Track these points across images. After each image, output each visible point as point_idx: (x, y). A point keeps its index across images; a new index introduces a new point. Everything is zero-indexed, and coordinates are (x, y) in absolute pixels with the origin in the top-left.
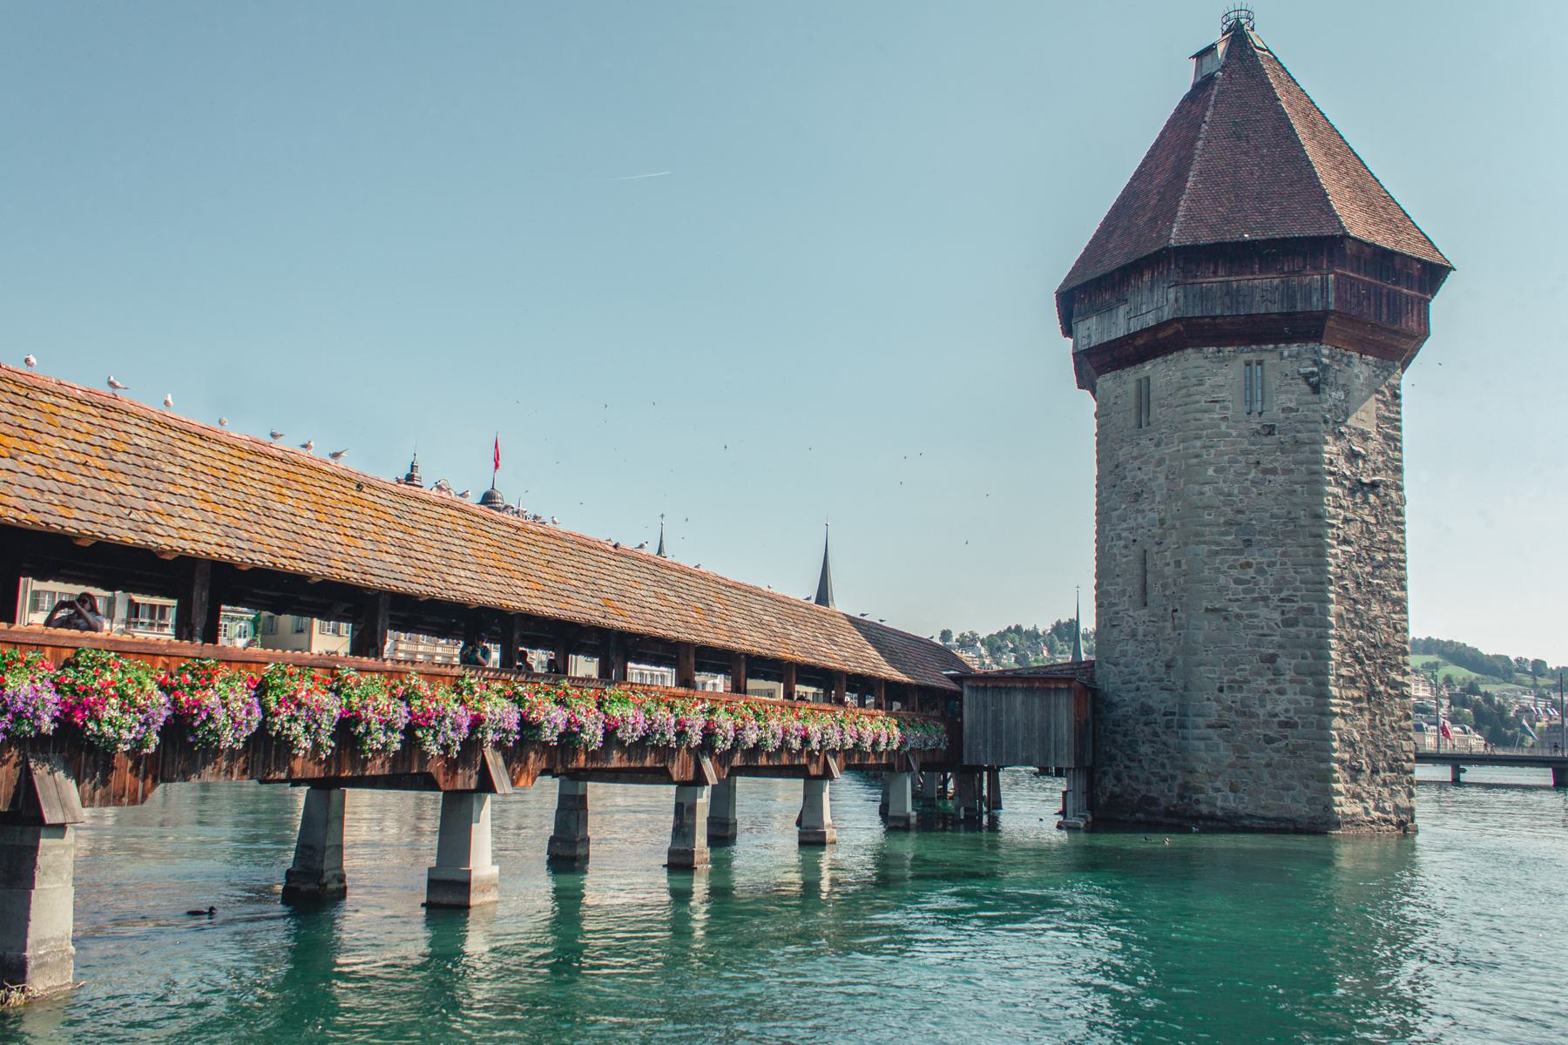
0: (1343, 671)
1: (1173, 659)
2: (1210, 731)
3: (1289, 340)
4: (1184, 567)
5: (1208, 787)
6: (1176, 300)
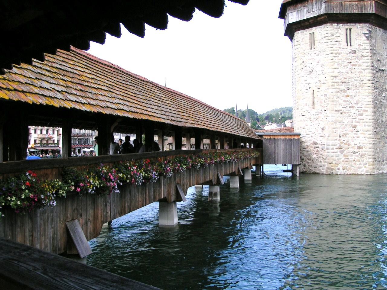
1: (324, 127)
2: (336, 150)
4: (328, 96)
6: (325, 7)
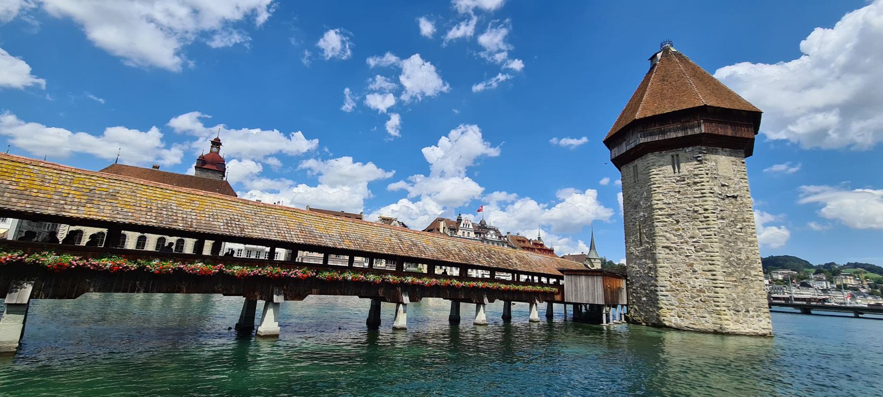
0: (725, 270)
3: (688, 146)
5: (667, 315)
